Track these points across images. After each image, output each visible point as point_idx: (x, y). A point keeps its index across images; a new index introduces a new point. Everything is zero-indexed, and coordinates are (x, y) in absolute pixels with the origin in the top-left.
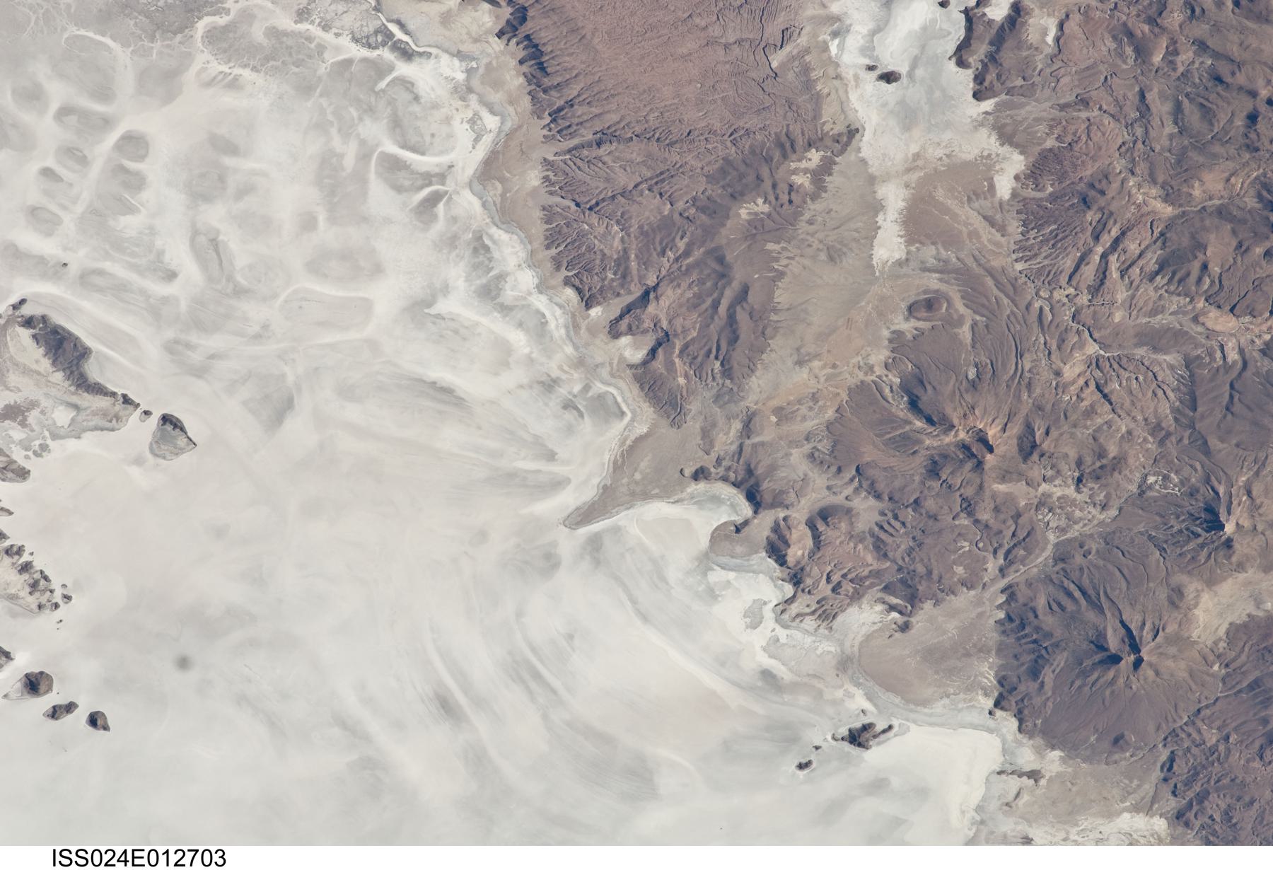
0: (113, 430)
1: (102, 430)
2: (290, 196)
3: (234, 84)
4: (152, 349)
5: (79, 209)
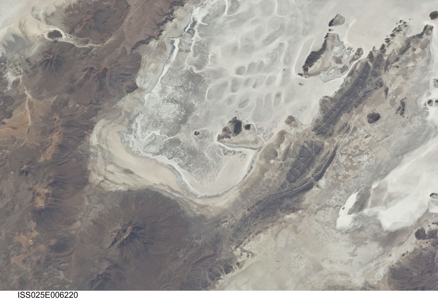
0: (338, 36)
1: (338, 38)
2: (247, 29)
3: (214, 57)
4: (308, 38)
5: (264, 74)
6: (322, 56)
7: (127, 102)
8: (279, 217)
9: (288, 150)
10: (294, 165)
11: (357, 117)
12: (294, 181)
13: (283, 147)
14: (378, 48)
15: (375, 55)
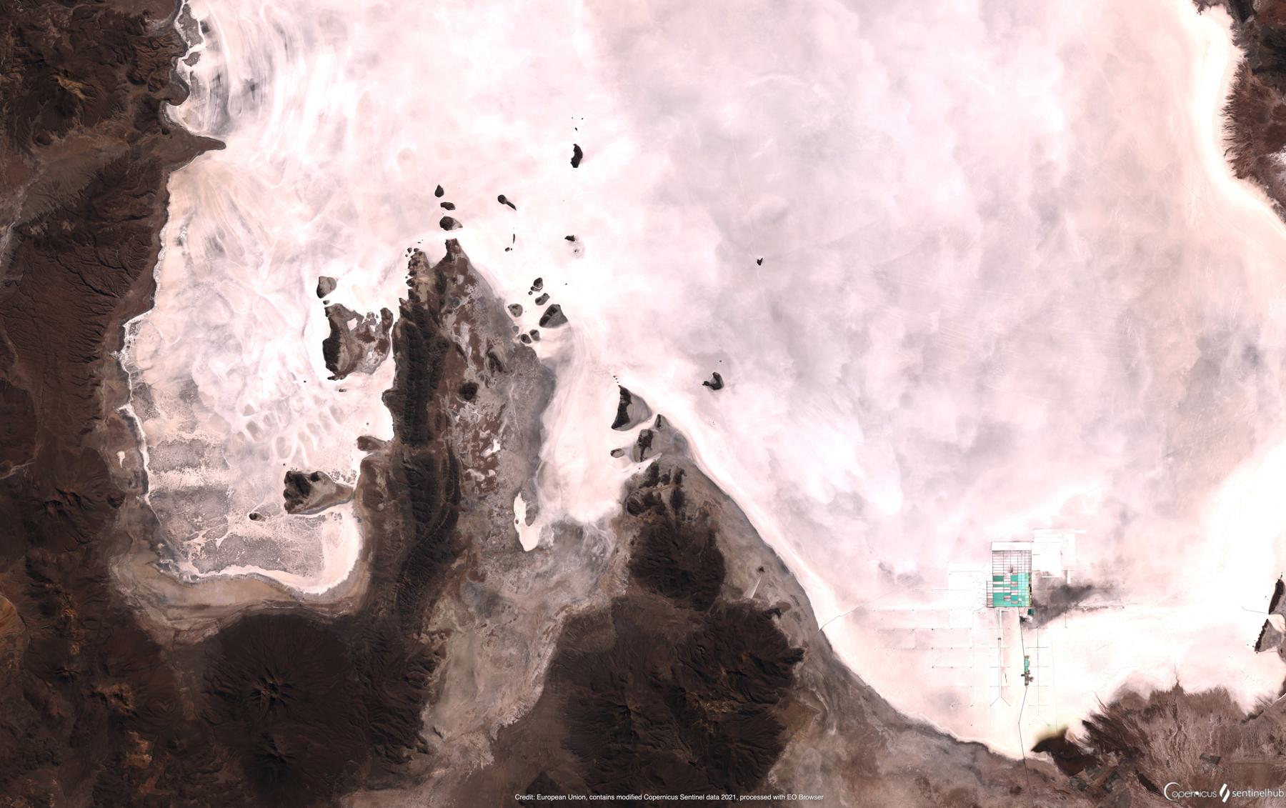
6: (342, 340)
7: (125, 517)
8: (444, 572)
9: (389, 483)
10: (413, 497)
11: (447, 400)
12: (428, 519)
13: (381, 481)
14: (406, 297)
15: (409, 309)
